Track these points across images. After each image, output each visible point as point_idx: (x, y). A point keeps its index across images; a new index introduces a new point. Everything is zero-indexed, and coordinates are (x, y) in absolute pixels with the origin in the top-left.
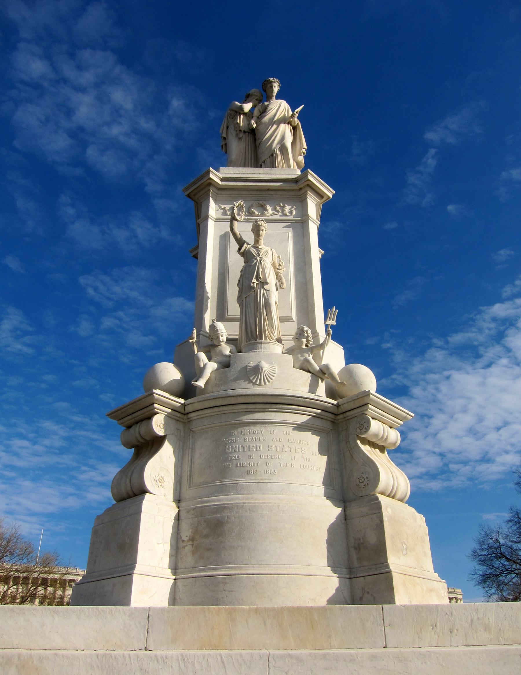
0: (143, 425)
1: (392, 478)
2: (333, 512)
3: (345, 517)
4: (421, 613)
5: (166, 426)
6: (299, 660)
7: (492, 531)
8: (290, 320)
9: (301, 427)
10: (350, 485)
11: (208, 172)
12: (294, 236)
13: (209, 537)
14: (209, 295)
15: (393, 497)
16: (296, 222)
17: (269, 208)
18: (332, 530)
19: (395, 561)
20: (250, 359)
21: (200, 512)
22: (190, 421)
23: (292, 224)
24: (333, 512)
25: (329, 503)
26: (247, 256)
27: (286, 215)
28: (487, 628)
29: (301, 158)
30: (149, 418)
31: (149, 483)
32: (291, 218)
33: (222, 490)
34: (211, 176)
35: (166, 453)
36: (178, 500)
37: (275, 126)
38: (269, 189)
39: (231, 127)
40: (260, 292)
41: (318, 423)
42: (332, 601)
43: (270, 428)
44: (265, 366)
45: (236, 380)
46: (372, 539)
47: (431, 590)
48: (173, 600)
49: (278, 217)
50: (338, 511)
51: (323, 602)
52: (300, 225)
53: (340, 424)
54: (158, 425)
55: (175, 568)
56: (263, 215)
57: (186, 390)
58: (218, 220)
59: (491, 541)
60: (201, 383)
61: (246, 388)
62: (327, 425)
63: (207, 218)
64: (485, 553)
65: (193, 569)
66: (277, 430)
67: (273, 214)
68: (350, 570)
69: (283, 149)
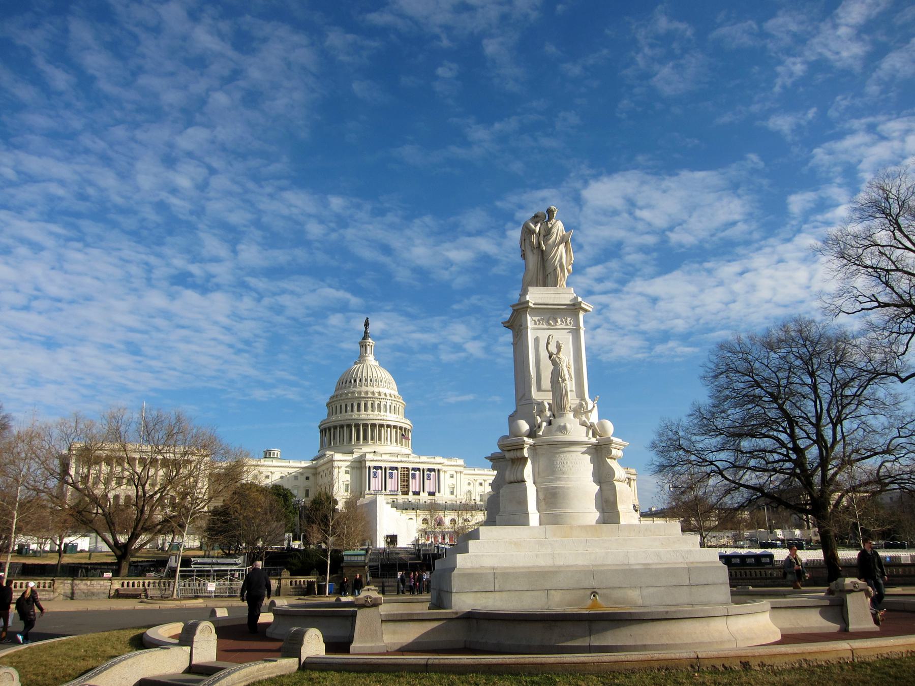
0: (519, 452)
1: (619, 472)
3: (601, 490)
4: (630, 527)
7: (672, 424)
9: (583, 453)
10: (603, 477)
13: (551, 499)
20: (561, 421)
21: (547, 489)
23: (571, 331)
26: (554, 363)
30: (523, 449)
32: (570, 327)
33: (553, 480)
39: (527, 241)
40: (563, 385)
41: (591, 450)
44: (568, 426)
46: (612, 499)
49: (563, 326)
52: (576, 332)
53: (600, 451)
54: (526, 453)
55: (538, 510)
57: (532, 434)
58: (532, 329)
59: (670, 433)
60: (541, 433)
61: (561, 437)
62: (592, 451)
63: (527, 328)
64: (664, 444)
68: (603, 509)
69: (562, 266)
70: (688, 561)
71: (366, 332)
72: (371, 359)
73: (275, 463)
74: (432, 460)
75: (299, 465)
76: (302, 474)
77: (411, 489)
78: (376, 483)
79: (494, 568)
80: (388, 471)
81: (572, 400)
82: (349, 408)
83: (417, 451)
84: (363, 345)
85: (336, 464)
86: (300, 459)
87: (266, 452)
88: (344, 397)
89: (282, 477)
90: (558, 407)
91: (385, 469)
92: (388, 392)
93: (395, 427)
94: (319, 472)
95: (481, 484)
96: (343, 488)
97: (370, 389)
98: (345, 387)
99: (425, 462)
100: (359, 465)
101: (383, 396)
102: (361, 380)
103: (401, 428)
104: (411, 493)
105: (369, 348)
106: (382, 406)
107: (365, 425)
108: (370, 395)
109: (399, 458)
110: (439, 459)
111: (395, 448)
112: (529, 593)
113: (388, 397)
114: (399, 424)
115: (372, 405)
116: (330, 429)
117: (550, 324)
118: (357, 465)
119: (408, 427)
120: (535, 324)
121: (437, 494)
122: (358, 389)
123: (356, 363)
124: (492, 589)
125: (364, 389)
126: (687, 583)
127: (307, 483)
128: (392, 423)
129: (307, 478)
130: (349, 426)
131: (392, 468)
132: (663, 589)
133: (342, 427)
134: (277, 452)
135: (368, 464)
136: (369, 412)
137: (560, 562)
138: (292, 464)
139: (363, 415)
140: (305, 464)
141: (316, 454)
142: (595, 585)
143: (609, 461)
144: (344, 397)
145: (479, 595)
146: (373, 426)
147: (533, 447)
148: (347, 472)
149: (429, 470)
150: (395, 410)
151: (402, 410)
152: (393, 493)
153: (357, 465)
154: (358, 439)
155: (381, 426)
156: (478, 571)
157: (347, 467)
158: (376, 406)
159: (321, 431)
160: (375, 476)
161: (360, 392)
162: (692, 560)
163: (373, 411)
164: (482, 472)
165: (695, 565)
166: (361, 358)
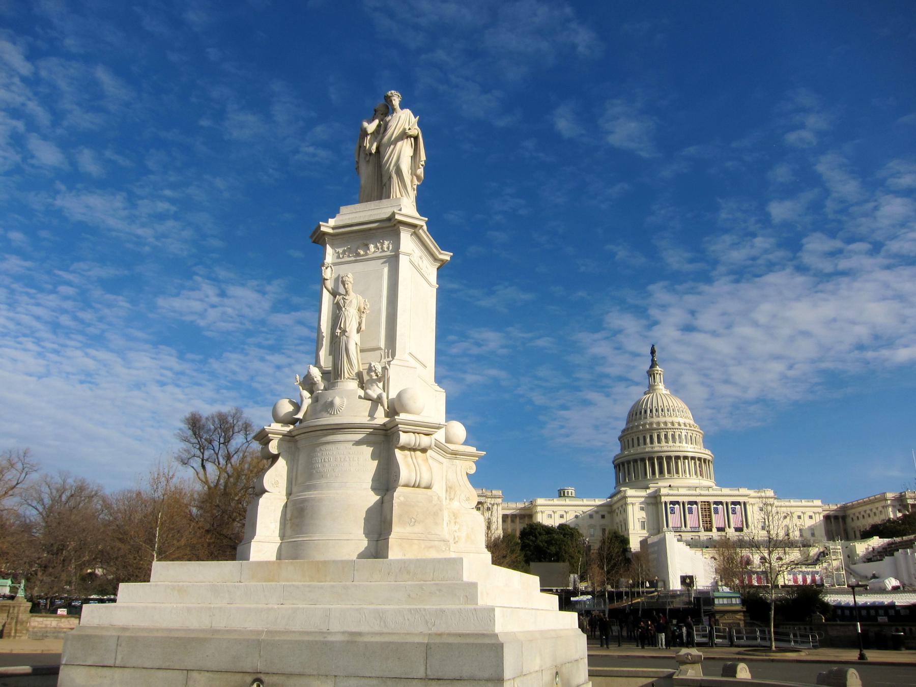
2: (374, 498)
5: (279, 446)
6: (298, 587)
8: (380, 349)
9: (358, 443)
11: (319, 226)
12: (389, 271)
14: (324, 334)
15: (418, 487)
16: (391, 256)
17: (372, 247)
18: (370, 512)
19: (397, 531)
21: (295, 502)
22: (296, 441)
24: (374, 498)
25: (372, 493)
27: (384, 251)
28: (408, 572)
29: (421, 171)
31: (266, 486)
32: (388, 253)
33: (309, 488)
34: (323, 229)
35: (281, 465)
36: (289, 494)
37: (392, 147)
38: (370, 229)
41: (372, 438)
42: (362, 556)
43: (338, 445)
44: (337, 401)
45: (321, 411)
47: (430, 547)
48: (279, 556)
49: (378, 254)
50: (378, 498)
51: (354, 557)
54: (273, 448)
55: (282, 536)
56: (366, 254)
60: (300, 416)
65: (291, 537)
66: (341, 446)
67: (375, 252)
70: (434, 630)
71: (653, 360)
72: (661, 388)
73: (568, 502)
74: (736, 492)
75: (592, 503)
76: (597, 512)
77: (714, 526)
78: (674, 520)
79: (124, 629)
80: (687, 506)
81: (356, 361)
82: (641, 441)
83: (720, 483)
84: (651, 374)
85: (629, 500)
86: (599, 497)
87: (560, 491)
88: (635, 430)
89: (576, 517)
90: (333, 376)
91: (683, 503)
92: (682, 421)
93: (693, 458)
94: (613, 510)
95: (799, 517)
96: (638, 526)
97: (662, 419)
98: (636, 420)
99: (727, 494)
100: (654, 501)
101: (676, 426)
102: (651, 411)
103: (700, 459)
104: (714, 530)
105: (657, 377)
106: (677, 437)
107: (660, 459)
108: (662, 426)
109: (698, 491)
110: (743, 491)
111: (694, 481)
112: (161, 673)
113: (683, 427)
114: (697, 455)
115: (666, 436)
116: (623, 464)
117: (358, 255)
118: (650, 501)
119: (710, 458)
120: (338, 257)
121: (745, 528)
122: (649, 420)
123: (645, 393)
124: (111, 663)
125: (655, 420)
126: (421, 674)
127: (603, 522)
128: (690, 454)
129: (603, 517)
130: (643, 460)
131: (691, 503)
132: (374, 682)
133: (635, 461)
134: (571, 491)
135: (663, 499)
136: (663, 443)
137: (221, 623)
138: (585, 502)
139: (657, 447)
140: (599, 502)
141: (613, 491)
142: (260, 666)
143: (397, 451)
144: (635, 430)
145: (93, 671)
146: (669, 458)
147: (289, 438)
148: (642, 509)
149: (734, 503)
150: (692, 440)
151: (700, 440)
152: (695, 530)
153: (650, 501)
154: (654, 473)
155: (677, 458)
156: (105, 633)
157: (641, 503)
158: (670, 437)
159: (615, 467)
160: (673, 512)
161: (651, 424)
162: (443, 629)
163: (667, 442)
164: (799, 504)
165: (446, 640)
166: (651, 388)
